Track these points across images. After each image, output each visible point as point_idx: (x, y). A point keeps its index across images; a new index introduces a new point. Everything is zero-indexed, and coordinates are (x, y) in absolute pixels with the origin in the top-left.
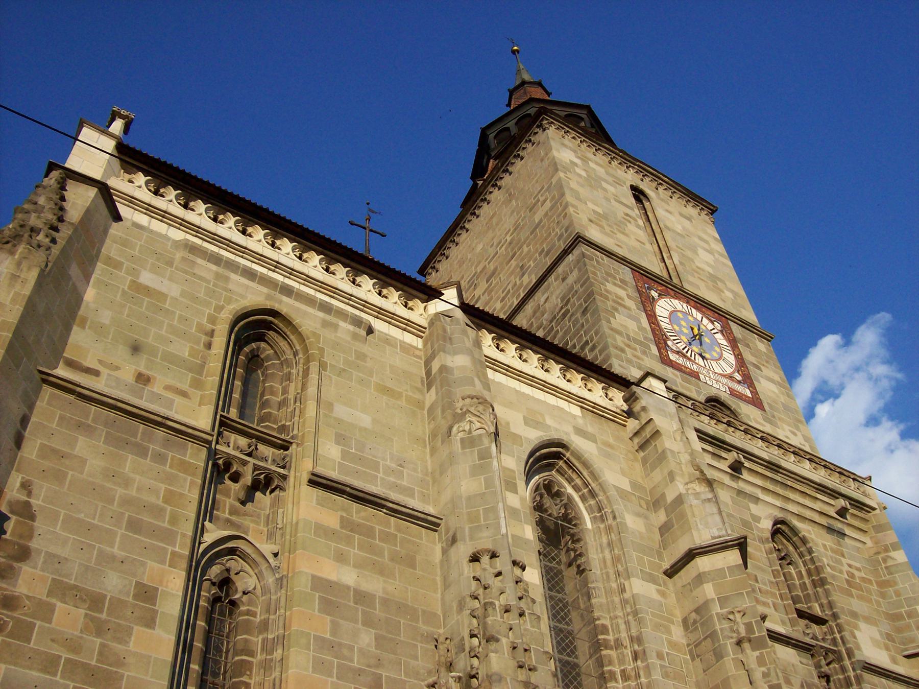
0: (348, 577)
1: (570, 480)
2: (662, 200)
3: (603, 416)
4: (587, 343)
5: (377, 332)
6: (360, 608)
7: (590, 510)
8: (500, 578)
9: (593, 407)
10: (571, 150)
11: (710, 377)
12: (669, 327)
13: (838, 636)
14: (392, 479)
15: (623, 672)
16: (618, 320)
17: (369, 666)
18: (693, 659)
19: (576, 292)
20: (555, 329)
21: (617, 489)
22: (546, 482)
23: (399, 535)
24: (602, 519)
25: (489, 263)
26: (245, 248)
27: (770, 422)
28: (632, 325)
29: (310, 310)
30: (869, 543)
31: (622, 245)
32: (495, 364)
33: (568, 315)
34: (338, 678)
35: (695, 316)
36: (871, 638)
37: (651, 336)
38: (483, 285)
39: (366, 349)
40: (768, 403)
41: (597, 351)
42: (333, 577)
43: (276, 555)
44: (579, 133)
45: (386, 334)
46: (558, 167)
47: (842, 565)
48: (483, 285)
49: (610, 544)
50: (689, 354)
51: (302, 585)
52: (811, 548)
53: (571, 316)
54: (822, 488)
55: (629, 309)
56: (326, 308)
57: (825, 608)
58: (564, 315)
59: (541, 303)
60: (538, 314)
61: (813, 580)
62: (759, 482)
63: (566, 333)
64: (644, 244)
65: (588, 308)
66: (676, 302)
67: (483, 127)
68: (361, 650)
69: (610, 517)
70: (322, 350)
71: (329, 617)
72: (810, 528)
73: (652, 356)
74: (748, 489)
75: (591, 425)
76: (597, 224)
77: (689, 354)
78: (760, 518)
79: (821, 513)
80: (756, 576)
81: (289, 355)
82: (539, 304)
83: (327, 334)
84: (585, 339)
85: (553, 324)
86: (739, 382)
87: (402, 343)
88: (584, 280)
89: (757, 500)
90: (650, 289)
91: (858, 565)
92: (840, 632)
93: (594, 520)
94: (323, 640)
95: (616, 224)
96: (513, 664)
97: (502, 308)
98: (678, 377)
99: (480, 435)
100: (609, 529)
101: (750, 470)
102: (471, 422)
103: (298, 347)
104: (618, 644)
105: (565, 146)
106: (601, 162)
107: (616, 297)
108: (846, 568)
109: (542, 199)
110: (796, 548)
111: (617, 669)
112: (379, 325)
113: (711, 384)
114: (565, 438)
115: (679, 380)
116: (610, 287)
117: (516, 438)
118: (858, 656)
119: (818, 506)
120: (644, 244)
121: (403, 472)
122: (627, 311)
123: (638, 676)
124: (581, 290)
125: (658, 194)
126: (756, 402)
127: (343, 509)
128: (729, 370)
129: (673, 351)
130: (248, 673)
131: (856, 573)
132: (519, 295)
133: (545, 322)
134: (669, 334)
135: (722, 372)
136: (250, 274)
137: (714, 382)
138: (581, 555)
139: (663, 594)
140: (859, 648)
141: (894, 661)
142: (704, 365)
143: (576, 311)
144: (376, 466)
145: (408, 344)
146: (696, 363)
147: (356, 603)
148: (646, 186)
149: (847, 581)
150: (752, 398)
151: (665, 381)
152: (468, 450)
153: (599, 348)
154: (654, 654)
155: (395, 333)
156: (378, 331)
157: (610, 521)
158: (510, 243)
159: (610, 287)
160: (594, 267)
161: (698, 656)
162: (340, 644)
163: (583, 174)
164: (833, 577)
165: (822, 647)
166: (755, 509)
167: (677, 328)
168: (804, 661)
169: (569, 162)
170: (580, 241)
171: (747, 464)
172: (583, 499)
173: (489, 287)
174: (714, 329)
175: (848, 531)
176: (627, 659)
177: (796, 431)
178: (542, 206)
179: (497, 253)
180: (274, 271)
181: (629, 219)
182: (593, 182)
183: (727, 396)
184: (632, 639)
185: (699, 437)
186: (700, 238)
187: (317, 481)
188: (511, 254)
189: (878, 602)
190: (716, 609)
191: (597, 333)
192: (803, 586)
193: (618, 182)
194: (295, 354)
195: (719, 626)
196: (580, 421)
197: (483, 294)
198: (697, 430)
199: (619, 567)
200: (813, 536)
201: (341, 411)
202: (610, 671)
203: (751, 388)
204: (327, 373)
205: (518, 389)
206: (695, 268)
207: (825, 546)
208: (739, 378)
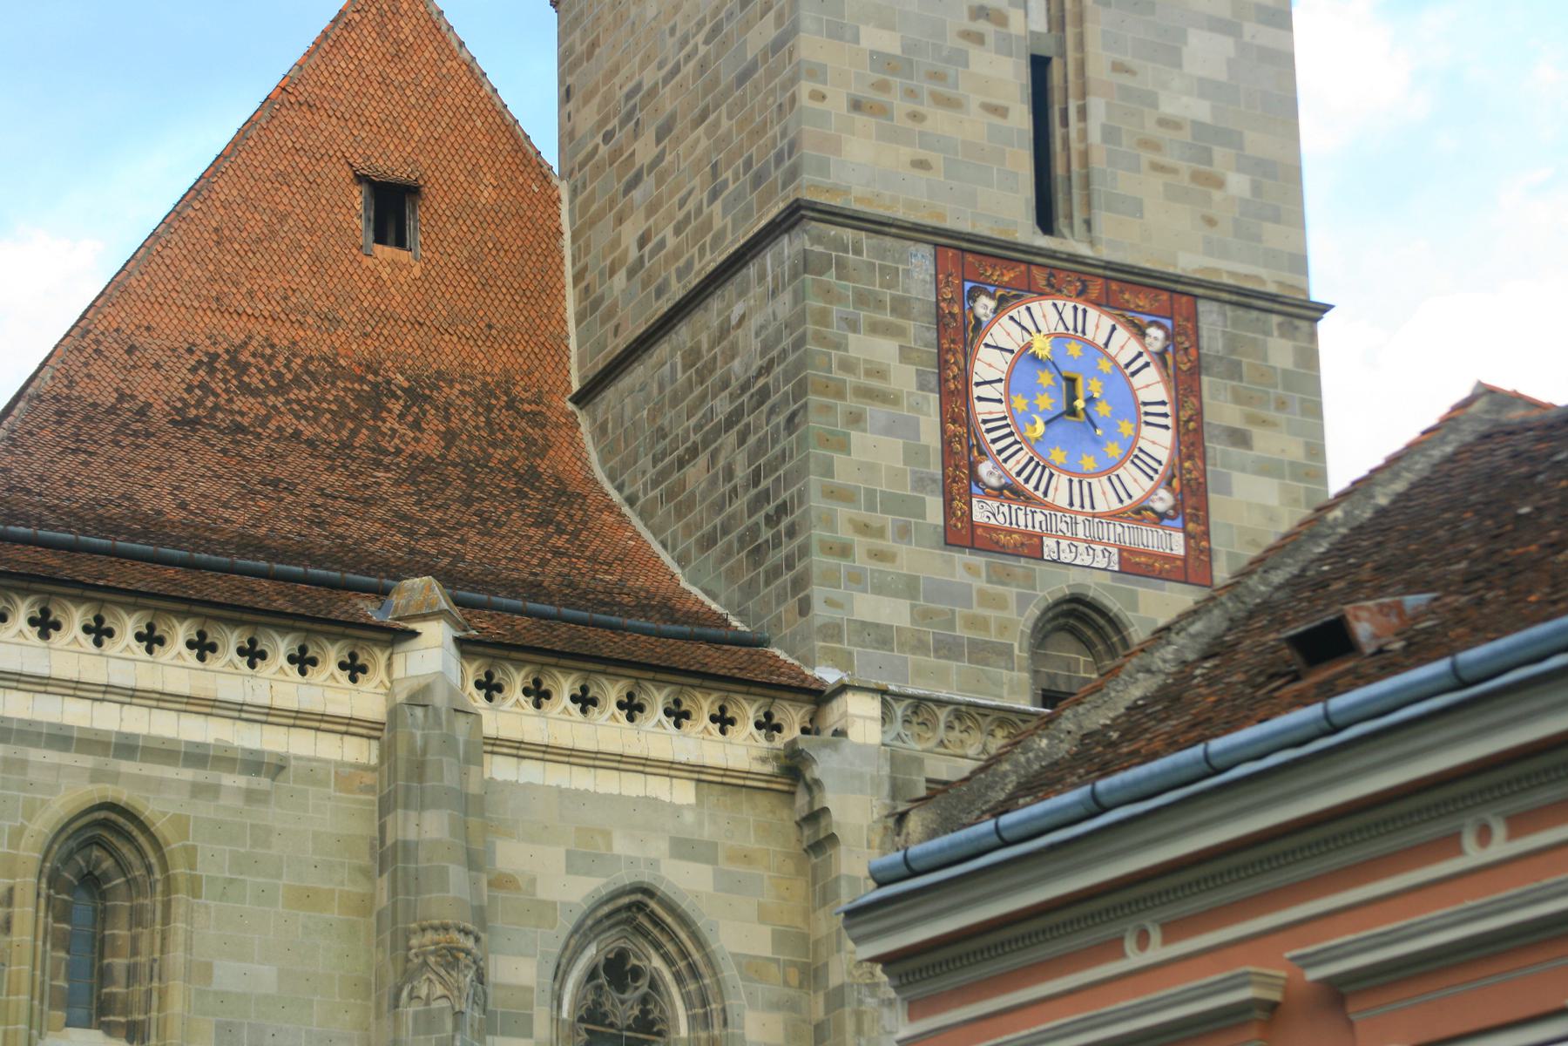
1: (657, 946)
5: (293, 762)
7: (687, 999)
11: (1074, 538)
16: (854, 456)
20: (745, 420)
22: (611, 956)
24: (706, 1020)
25: (666, 81)
26: (49, 678)
32: (519, 749)
37: (936, 469)
45: (309, 759)
50: (1030, 486)
56: (197, 756)
65: (797, 420)
69: (717, 1020)
70: (191, 852)
81: (138, 872)
82: (729, 317)
83: (203, 809)
85: (745, 398)
90: (973, 295)
93: (692, 1019)
97: (676, 254)
99: (442, 1010)
102: (430, 980)
103: (153, 859)
114: (645, 876)
115: (980, 583)
117: (544, 910)
122: (887, 409)
124: (791, 358)
132: (702, 251)
133: (734, 384)
136: (61, 738)
137: (1082, 546)
152: (422, 1037)
157: (716, 1032)
167: (1020, 403)
174: (1140, 354)
178: (761, 18)
179: (676, 70)
180: (102, 700)
183: (1106, 578)
188: (701, 105)
194: (149, 869)
196: (689, 817)
201: (227, 975)
203: (1191, 526)
204: (203, 901)
206: (1152, 130)
208: (1163, 501)
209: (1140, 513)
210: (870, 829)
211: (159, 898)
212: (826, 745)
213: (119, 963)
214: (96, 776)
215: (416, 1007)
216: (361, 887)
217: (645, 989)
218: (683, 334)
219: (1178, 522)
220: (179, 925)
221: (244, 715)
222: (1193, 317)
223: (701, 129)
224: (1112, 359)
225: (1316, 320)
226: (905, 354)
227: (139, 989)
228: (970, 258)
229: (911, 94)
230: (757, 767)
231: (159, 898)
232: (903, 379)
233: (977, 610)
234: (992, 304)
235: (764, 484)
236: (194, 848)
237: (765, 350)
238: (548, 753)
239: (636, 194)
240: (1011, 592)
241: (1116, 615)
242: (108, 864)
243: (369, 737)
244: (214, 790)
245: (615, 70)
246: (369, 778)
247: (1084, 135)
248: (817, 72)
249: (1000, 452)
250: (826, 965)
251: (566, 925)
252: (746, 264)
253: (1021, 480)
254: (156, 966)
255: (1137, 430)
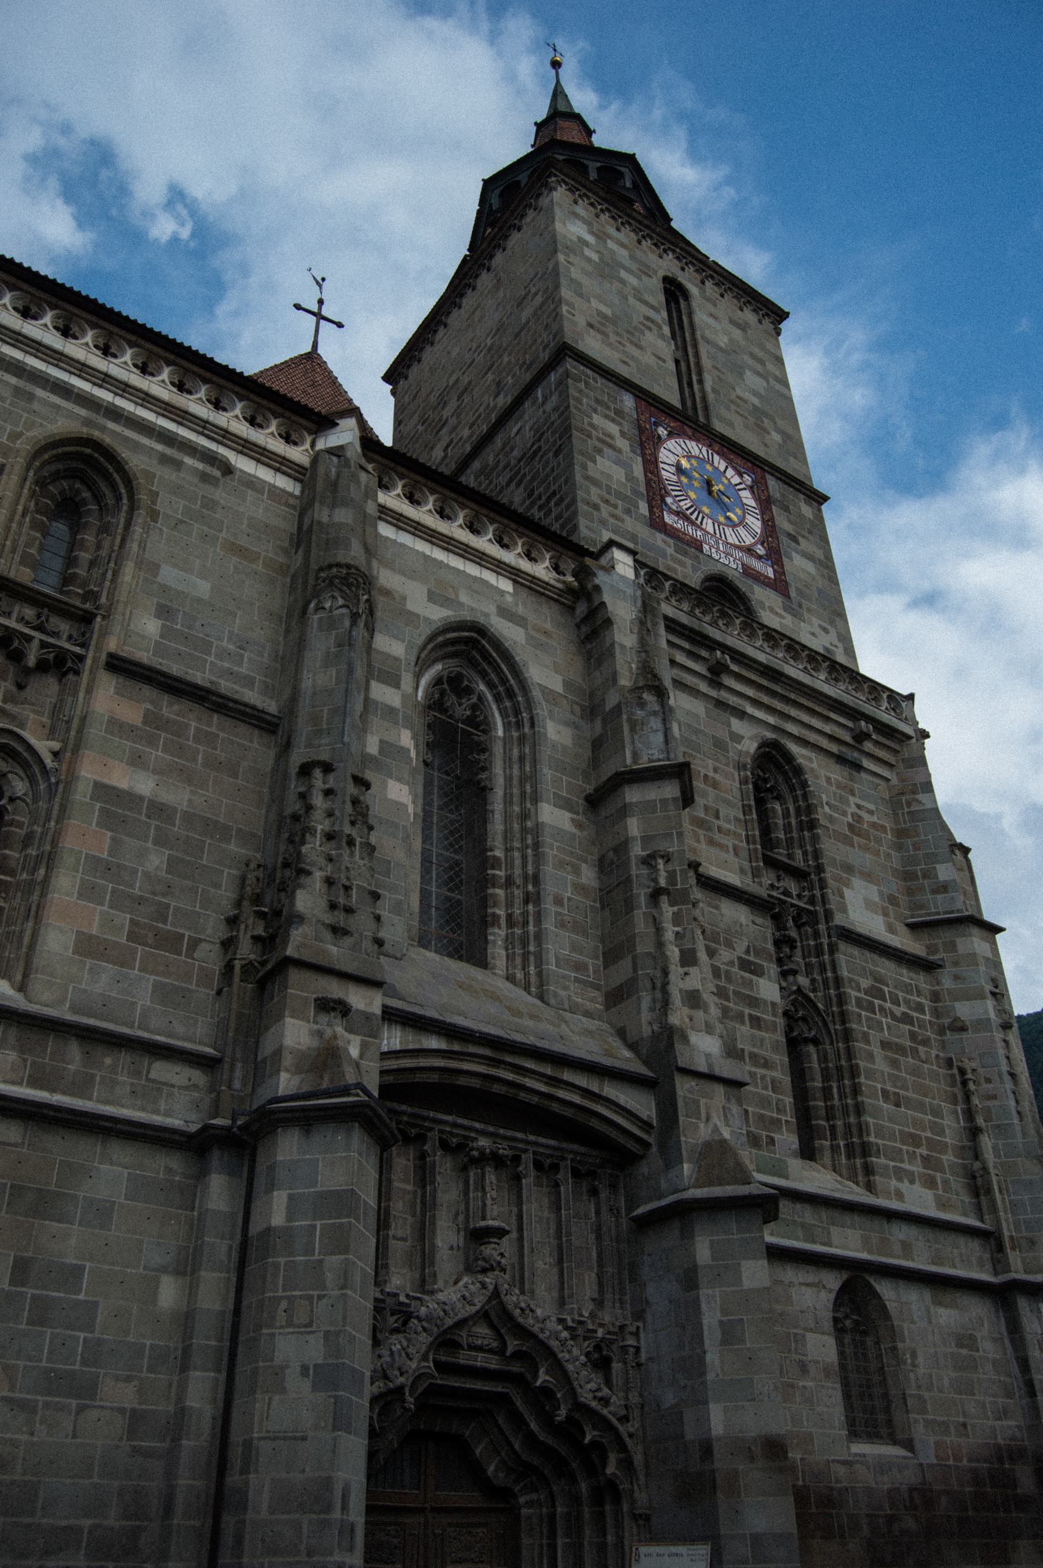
0: (144, 785)
1: (483, 675)
2: (708, 300)
3: (543, 594)
4: (554, 494)
5: (238, 473)
6: (154, 823)
8: (331, 797)
9: (531, 582)
10: (584, 223)
11: (718, 549)
12: (675, 478)
13: (817, 893)
14: (226, 665)
15: (509, 917)
17: (154, 893)
18: (603, 908)
19: (553, 423)
20: (522, 472)
21: (544, 689)
22: (452, 675)
23: (222, 735)
24: (519, 725)
25: (464, 373)
27: (795, 614)
28: (618, 474)
29: (145, 441)
30: (895, 781)
31: (632, 363)
32: (400, 521)
33: (540, 454)
34: (111, 907)
35: (716, 464)
36: (866, 900)
37: (642, 489)
38: (453, 404)
39: (219, 494)
40: (797, 589)
41: (563, 506)
42: (123, 784)
43: (56, 754)
44: (600, 197)
45: (250, 475)
46: (560, 247)
47: (849, 805)
48: (453, 404)
49: (522, 759)
50: (694, 517)
51: (82, 792)
52: (806, 780)
53: (542, 457)
54: (837, 706)
55: (619, 451)
57: (810, 858)
58: (535, 453)
59: (513, 435)
60: (507, 449)
61: (801, 821)
62: (750, 692)
63: (533, 479)
64: (664, 361)
66: (694, 447)
67: (486, 177)
68: (146, 874)
71: (109, 834)
72: (813, 755)
73: (639, 517)
74: (733, 700)
75: (525, 606)
76: (598, 331)
77: (694, 517)
78: (743, 737)
79: (832, 738)
80: (718, 811)
81: (110, 501)
84: (553, 488)
86: (760, 557)
87: (273, 487)
88: (564, 410)
89: (742, 715)
90: (656, 424)
91: (871, 807)
92: (822, 888)
93: (507, 726)
94: (99, 860)
95: (629, 332)
96: (323, 903)
97: (471, 436)
98: (670, 546)
99: (343, 615)
100: (522, 740)
101: (739, 677)
102: (333, 597)
103: (123, 491)
104: (509, 882)
105: (576, 216)
106: (626, 241)
107: (604, 434)
108: (853, 809)
109: (533, 290)
110: (787, 779)
111: (501, 912)
112: (244, 464)
113: (717, 558)
114: (482, 620)
115: (670, 551)
116: (597, 419)
117: (412, 618)
118: (838, 920)
119: (828, 728)
120: (664, 361)
121: (242, 656)
122: (615, 453)
123: (526, 923)
125: (702, 291)
126: (780, 585)
127: (152, 702)
128: (749, 540)
129: (671, 511)
130: (3, 895)
131: (866, 816)
133: (513, 462)
134: (670, 487)
135: (737, 543)
137: (723, 555)
138: (484, 769)
139: (579, 825)
140: (844, 909)
141: (891, 929)
142: (712, 532)
143: (549, 450)
144: (206, 646)
145: (281, 489)
146: (702, 529)
147: (149, 817)
148: (688, 280)
149: (850, 825)
150: (775, 579)
151: (633, 553)
153: (566, 502)
154: (551, 898)
155: (265, 474)
156: (241, 471)
157: (526, 730)
158: (489, 350)
159: (597, 419)
160: (580, 391)
161: (608, 905)
162: (119, 866)
163: (595, 257)
164: (831, 819)
165: (793, 905)
166: (737, 725)
168: (759, 920)
169: (575, 239)
170: (566, 354)
171: (734, 667)
172: (498, 699)
173: (459, 406)
174: (740, 484)
175: (866, 763)
176: (517, 901)
177: (829, 627)
180: (101, 386)
181: (651, 325)
182: (607, 270)
184: (525, 877)
185: (668, 628)
186: (753, 356)
187: (118, 665)
188: (489, 364)
189: (888, 855)
190: (637, 850)
191: (566, 482)
192: (788, 828)
193: (646, 271)
194: (119, 498)
195: (636, 871)
196: (509, 599)
197: (452, 415)
198: (666, 618)
199: (528, 788)
200: (815, 765)
201: (168, 575)
202: (494, 915)
205: (428, 553)
207: (828, 779)
208: (761, 550)
209: (749, 550)
210: (632, 622)
211: (123, 514)
212: (603, 568)
213: (85, 556)
214: (87, 422)
215: (321, 614)
216: (281, 559)
217: (474, 700)
218: (476, 465)
219: (769, 562)
220: (137, 528)
221: (206, 432)
222: (764, 478)
223: (489, 375)
224: (729, 480)
225: (822, 504)
226: (623, 434)
227: (97, 572)
228: (653, 409)
229: (618, 334)
230: (552, 582)
231: (123, 514)
232: (623, 444)
233: (670, 563)
234: (666, 432)
235: (536, 493)
236: (157, 494)
237: (537, 431)
238: (418, 529)
239: (445, 430)
240: (689, 562)
241: (744, 594)
242: (86, 494)
243: (295, 479)
244: (178, 465)
245: (432, 391)
246: (291, 501)
247: (703, 391)
248: (571, 305)
249: (677, 496)
250: (604, 700)
251: (426, 631)
252: (523, 403)
253: (688, 512)
254: (114, 555)
255: (744, 513)
